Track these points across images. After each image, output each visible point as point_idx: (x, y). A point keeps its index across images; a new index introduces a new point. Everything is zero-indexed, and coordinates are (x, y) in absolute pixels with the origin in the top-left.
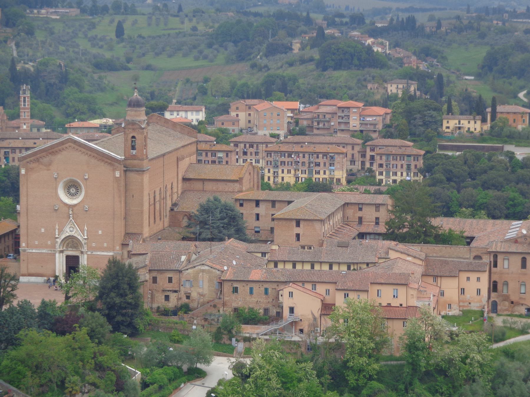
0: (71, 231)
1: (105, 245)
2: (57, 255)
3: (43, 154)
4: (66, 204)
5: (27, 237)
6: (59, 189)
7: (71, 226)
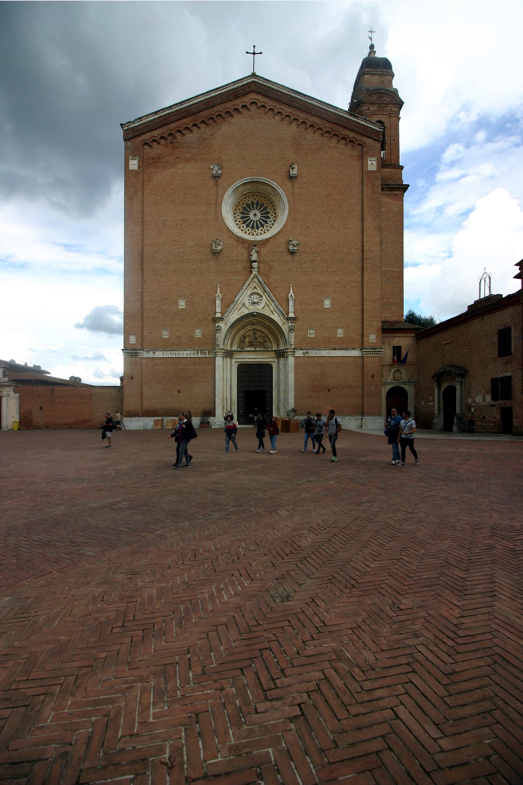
0: (254, 303)
1: (340, 332)
2: (219, 361)
3: (184, 120)
4: (243, 241)
6: (223, 205)
7: (255, 291)
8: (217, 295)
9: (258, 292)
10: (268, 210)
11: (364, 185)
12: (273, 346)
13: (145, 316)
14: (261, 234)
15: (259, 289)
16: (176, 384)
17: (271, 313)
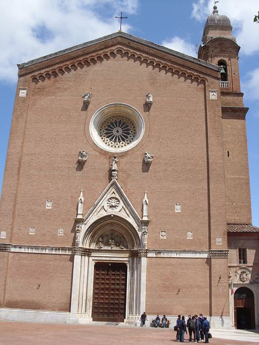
0: (111, 207)
5: (13, 218)
7: (113, 195)
8: (80, 198)
9: (116, 197)
10: (129, 127)
11: (207, 110)
12: (129, 246)
13: (17, 215)
14: (122, 146)
15: (117, 194)
16: (37, 278)
17: (127, 216)
